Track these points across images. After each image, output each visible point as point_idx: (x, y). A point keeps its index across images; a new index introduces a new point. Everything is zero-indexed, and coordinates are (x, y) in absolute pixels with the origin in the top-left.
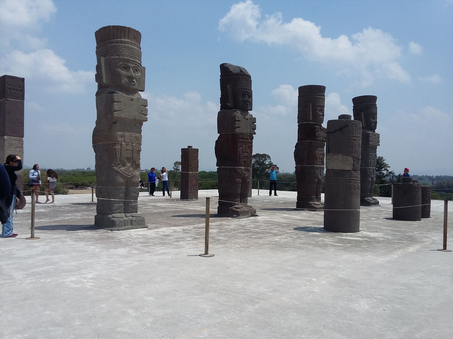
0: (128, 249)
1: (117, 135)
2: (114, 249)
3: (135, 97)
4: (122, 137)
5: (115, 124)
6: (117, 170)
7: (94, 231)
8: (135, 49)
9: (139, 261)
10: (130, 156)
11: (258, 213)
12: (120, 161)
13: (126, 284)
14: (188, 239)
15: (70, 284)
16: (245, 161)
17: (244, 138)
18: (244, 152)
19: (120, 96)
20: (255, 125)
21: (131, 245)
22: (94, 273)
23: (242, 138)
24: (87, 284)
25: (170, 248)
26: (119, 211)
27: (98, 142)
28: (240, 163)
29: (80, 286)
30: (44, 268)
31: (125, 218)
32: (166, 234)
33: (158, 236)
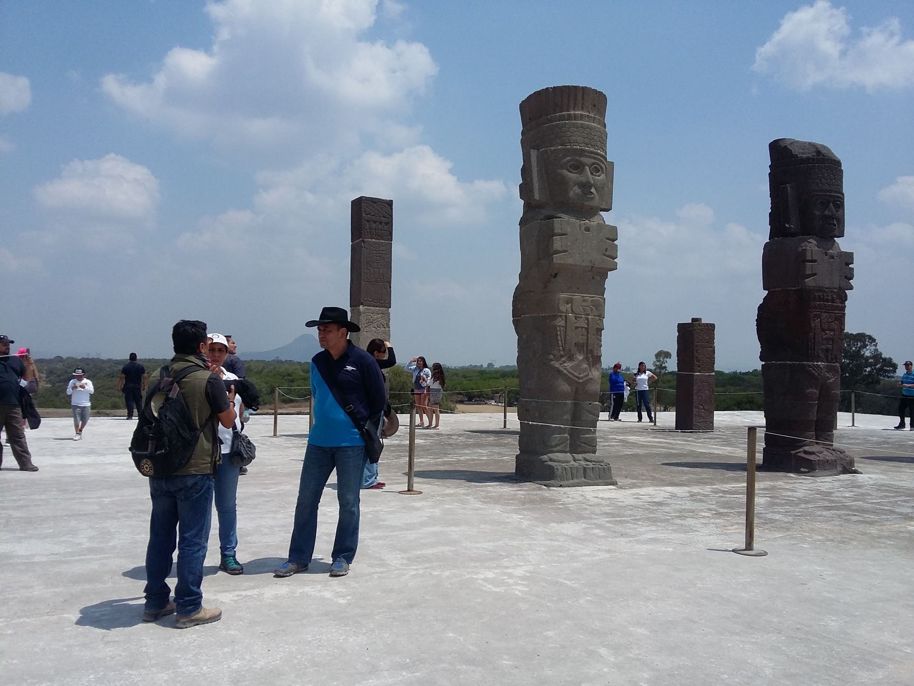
0: (584, 525)
1: (559, 299)
2: (557, 522)
3: (594, 222)
4: (568, 303)
5: (555, 279)
6: (558, 368)
7: (515, 486)
8: (595, 128)
9: (609, 551)
10: (581, 339)
11: (858, 467)
12: (564, 350)
13: (589, 596)
14: (703, 514)
15: (485, 584)
16: (827, 350)
17: (826, 298)
18: (824, 330)
19: (565, 222)
20: (850, 270)
21: (587, 518)
22: (525, 568)
23: (820, 299)
24: (515, 587)
25: (669, 530)
26: (561, 449)
27: (523, 314)
28: (816, 354)
29: (503, 591)
30: (435, 550)
31: (573, 462)
32: (657, 500)
33: (641, 503)
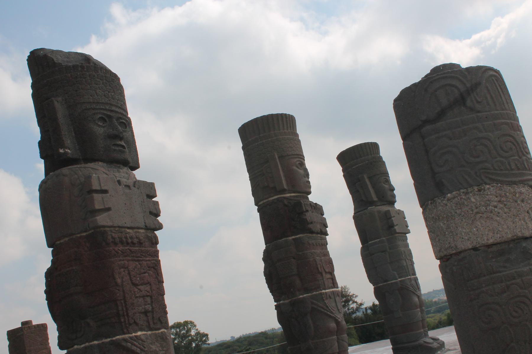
16: (146, 313)
28: (132, 321)
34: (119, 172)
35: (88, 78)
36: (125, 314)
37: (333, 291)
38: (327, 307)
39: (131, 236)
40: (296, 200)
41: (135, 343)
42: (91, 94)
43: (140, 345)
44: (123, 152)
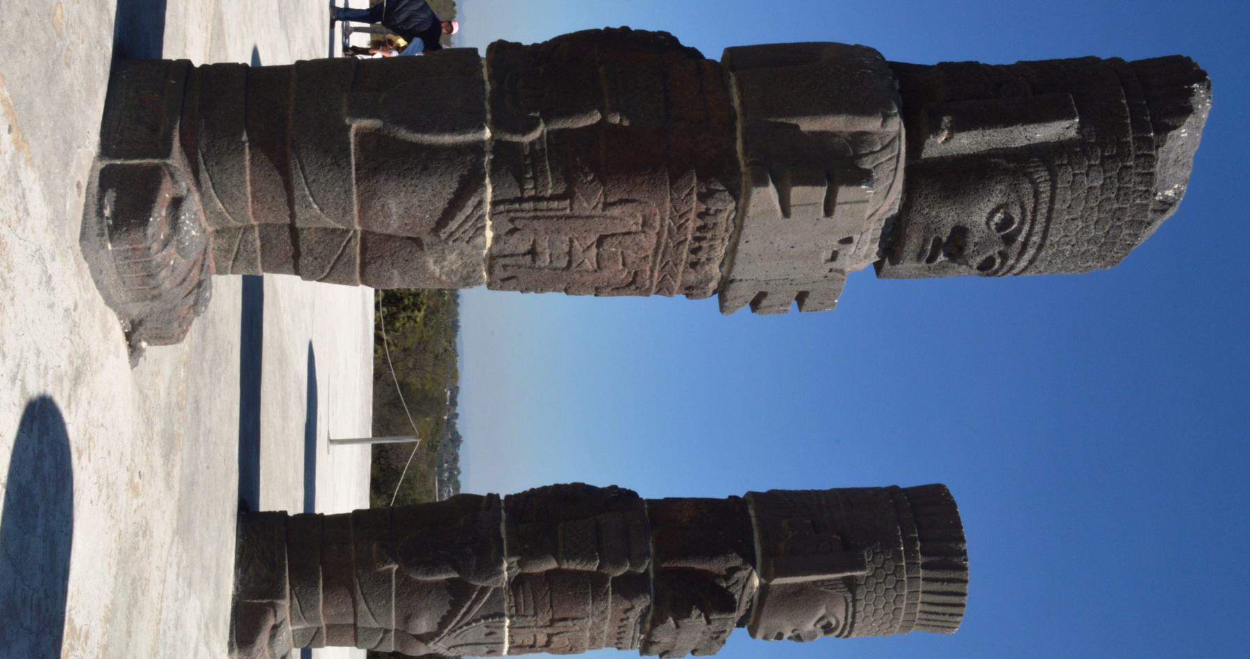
16: (533, 252)
28: (519, 224)
34: (873, 241)
35: (1116, 206)
36: (539, 214)
37: (502, 643)
38: (468, 624)
39: (714, 249)
40: (740, 599)
41: (470, 224)
42: (1074, 207)
43: (463, 233)
44: (919, 258)
